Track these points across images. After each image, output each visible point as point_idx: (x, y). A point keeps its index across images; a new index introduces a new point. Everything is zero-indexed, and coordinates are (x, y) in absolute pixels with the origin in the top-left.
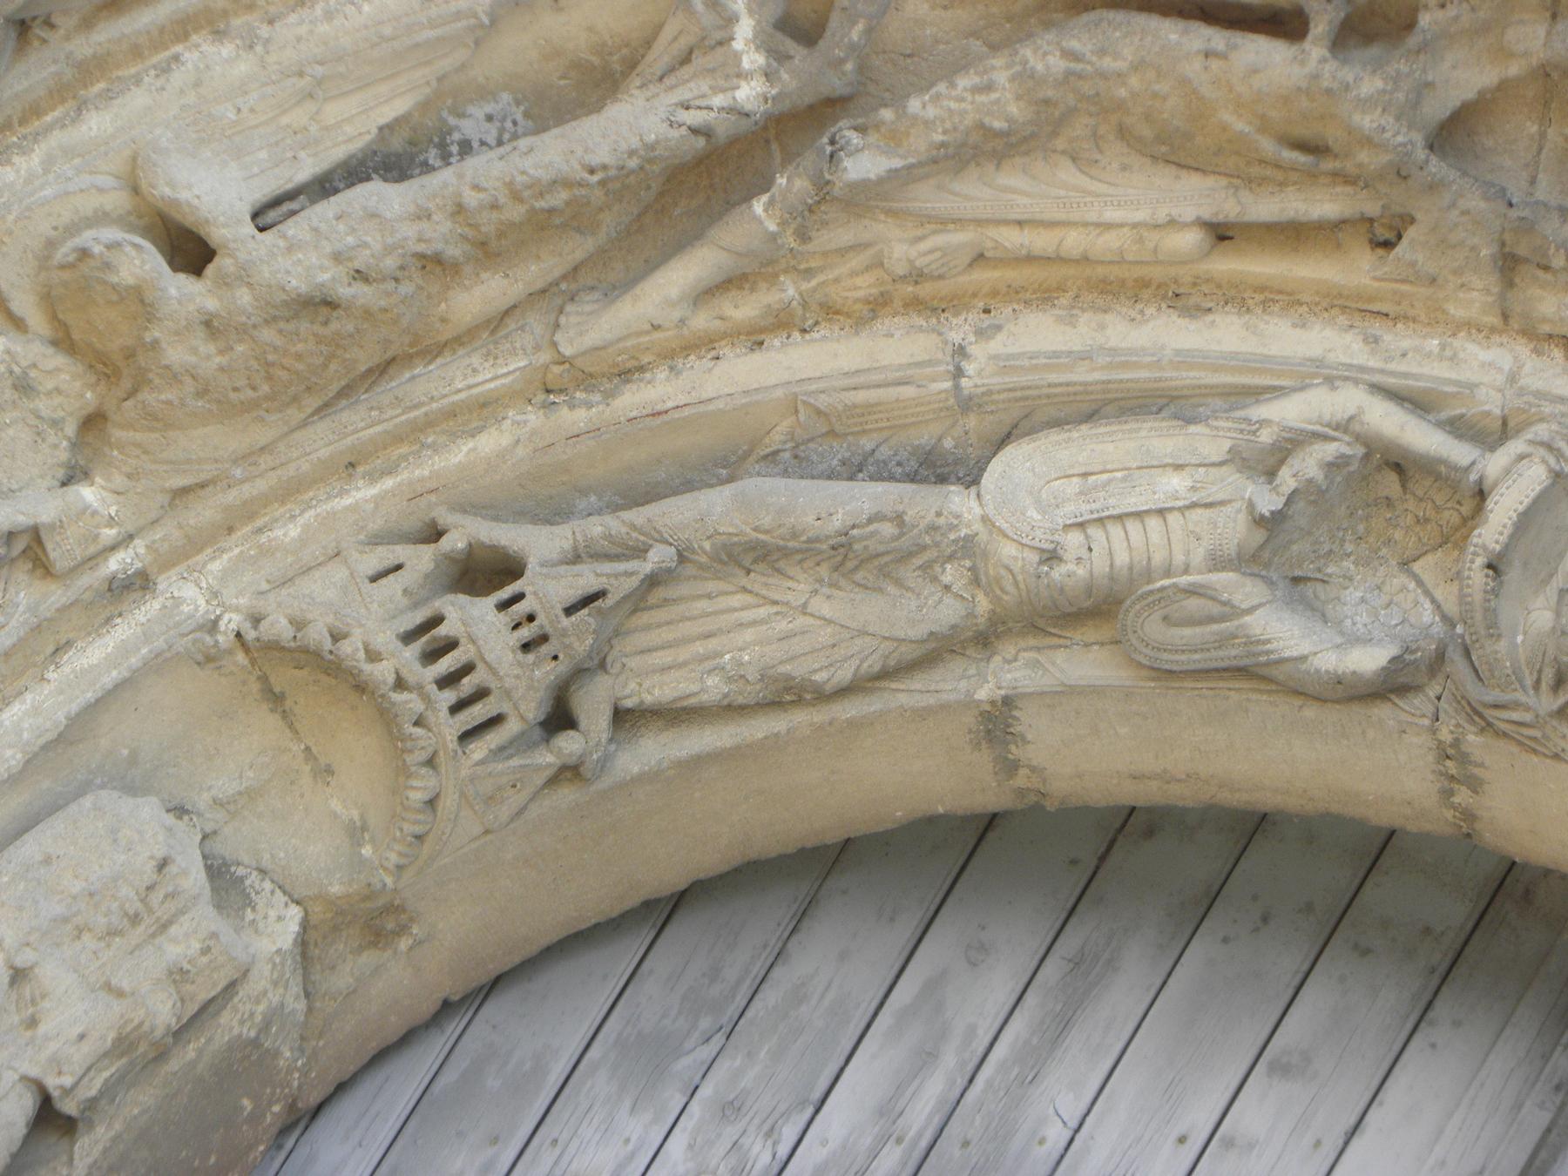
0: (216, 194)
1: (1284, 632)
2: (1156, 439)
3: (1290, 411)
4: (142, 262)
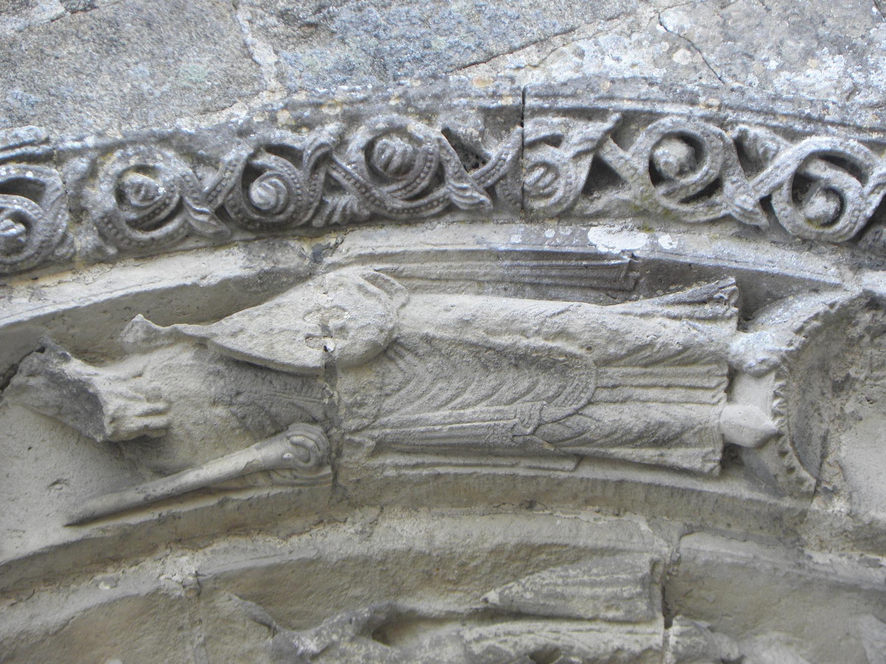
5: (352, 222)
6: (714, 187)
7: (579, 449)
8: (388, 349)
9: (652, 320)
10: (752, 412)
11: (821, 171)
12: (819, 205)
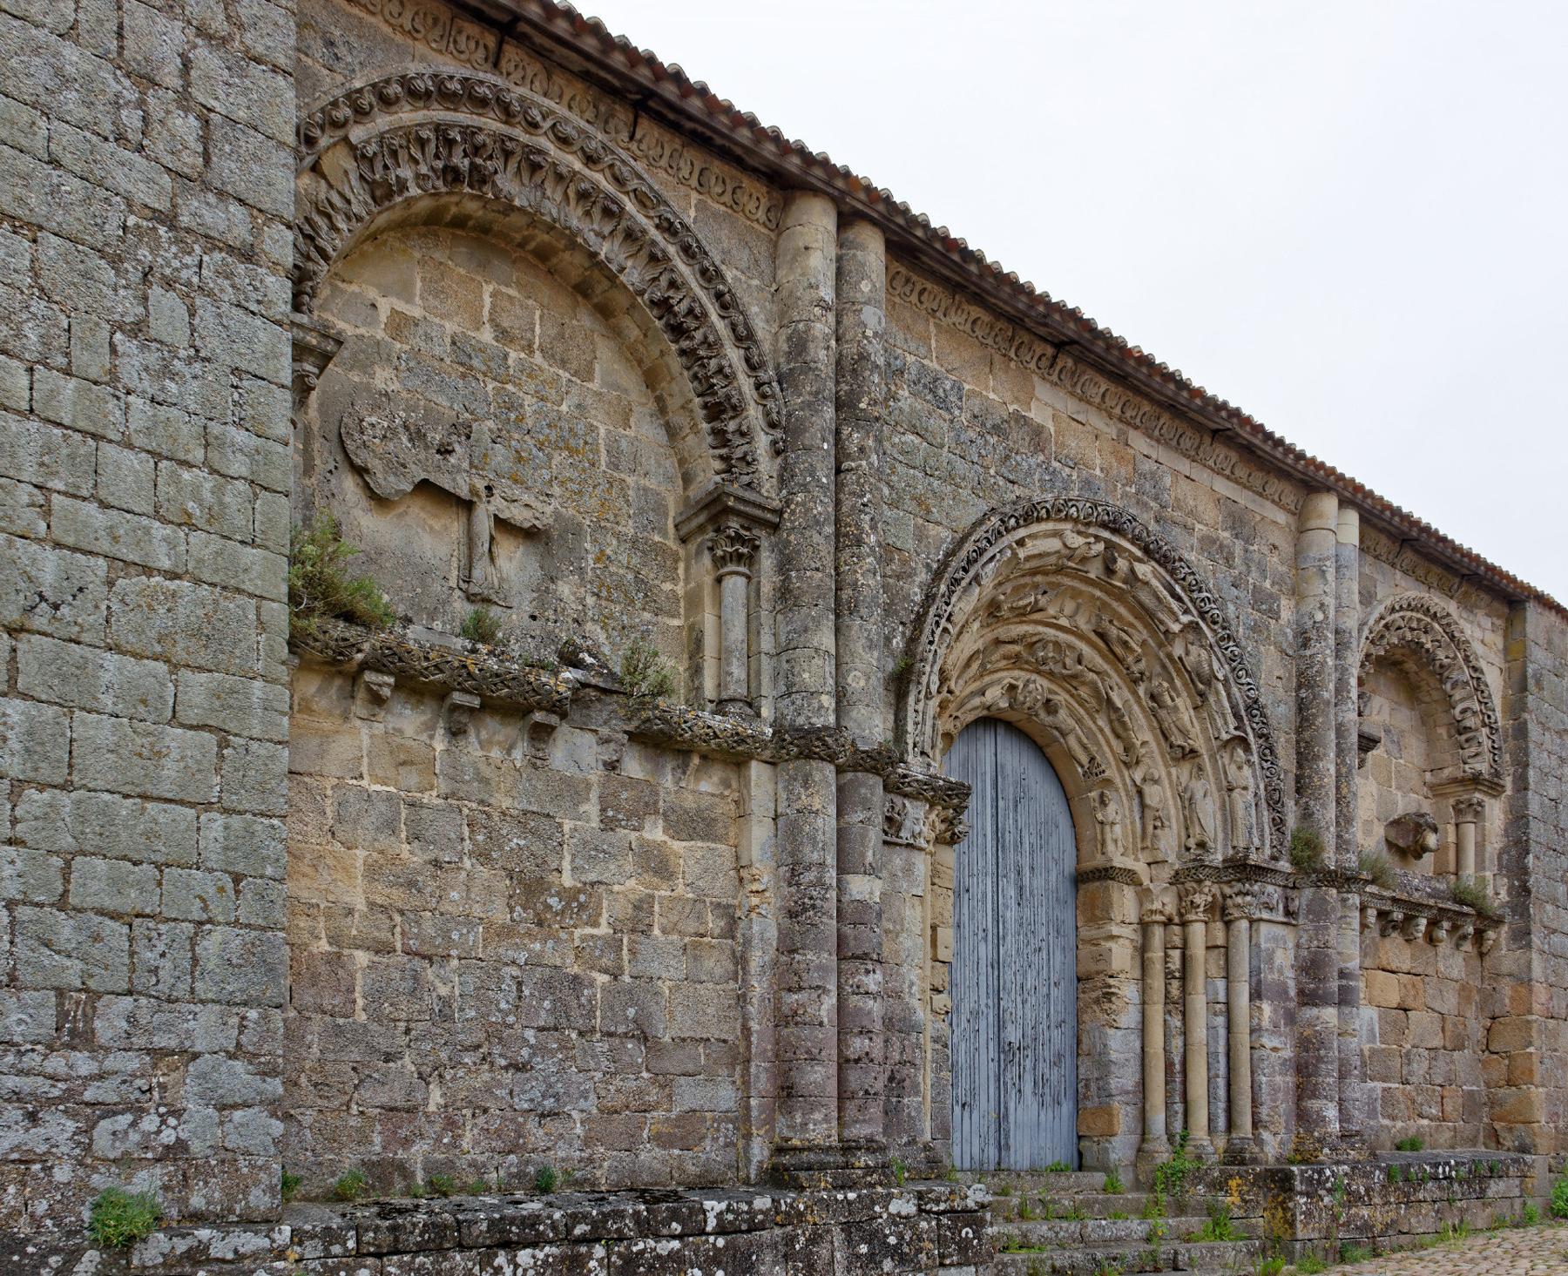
7: (1152, 615)
8: (1147, 583)
9: (1174, 605)
10: (1176, 628)
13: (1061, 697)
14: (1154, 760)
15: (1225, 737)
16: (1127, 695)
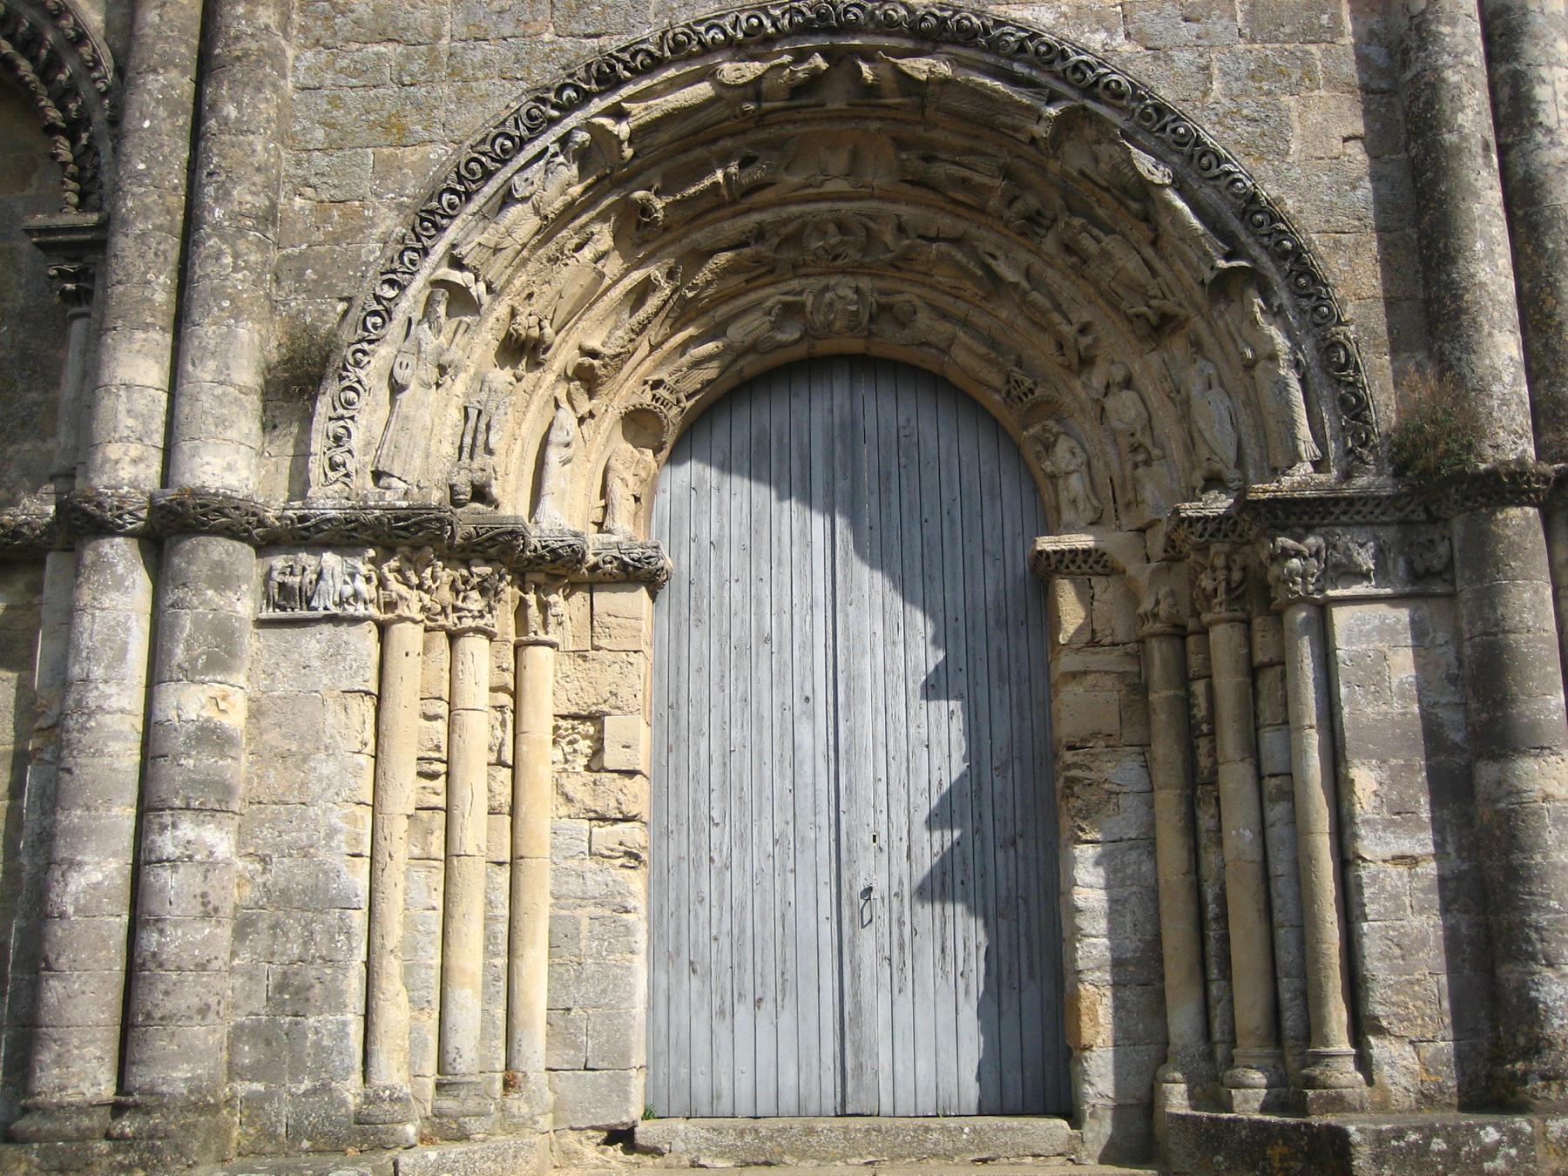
0: (594, 343)
1: (782, 337)
2: (750, 318)
3: (769, 303)
4: (588, 360)
5: (947, 42)
6: (1051, 62)
10: (1042, 130)
11: (1082, 66)
12: (1078, 76)
13: (908, 294)
14: (1118, 350)
15: (1209, 276)
16: (1023, 257)
